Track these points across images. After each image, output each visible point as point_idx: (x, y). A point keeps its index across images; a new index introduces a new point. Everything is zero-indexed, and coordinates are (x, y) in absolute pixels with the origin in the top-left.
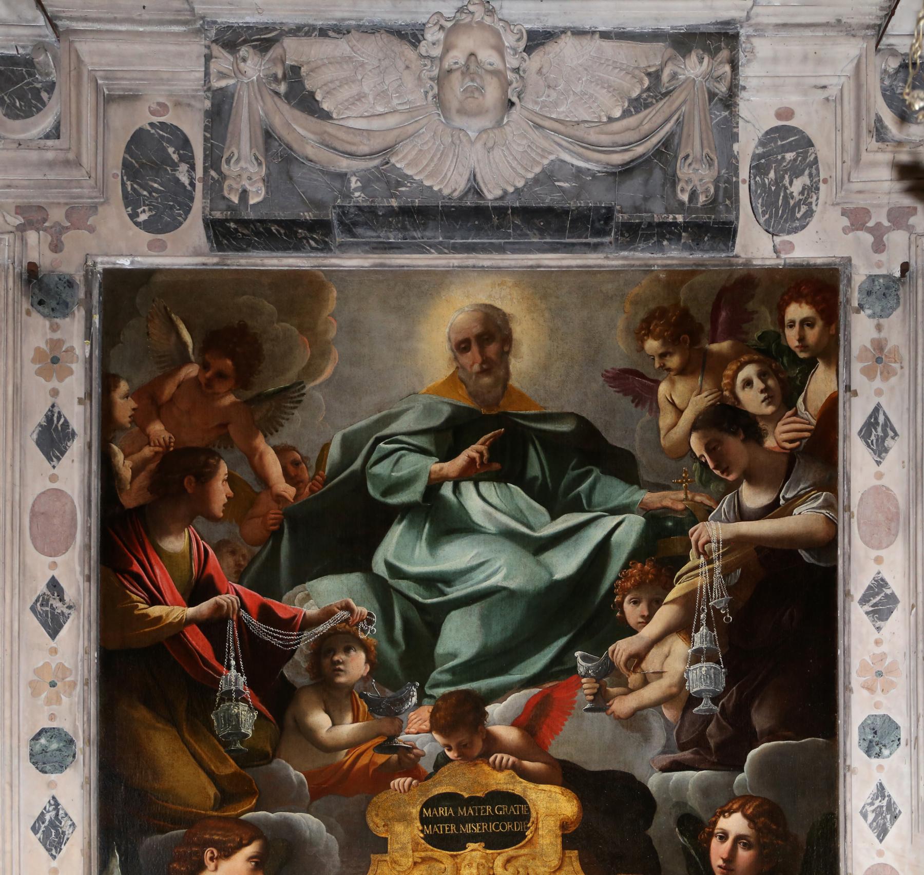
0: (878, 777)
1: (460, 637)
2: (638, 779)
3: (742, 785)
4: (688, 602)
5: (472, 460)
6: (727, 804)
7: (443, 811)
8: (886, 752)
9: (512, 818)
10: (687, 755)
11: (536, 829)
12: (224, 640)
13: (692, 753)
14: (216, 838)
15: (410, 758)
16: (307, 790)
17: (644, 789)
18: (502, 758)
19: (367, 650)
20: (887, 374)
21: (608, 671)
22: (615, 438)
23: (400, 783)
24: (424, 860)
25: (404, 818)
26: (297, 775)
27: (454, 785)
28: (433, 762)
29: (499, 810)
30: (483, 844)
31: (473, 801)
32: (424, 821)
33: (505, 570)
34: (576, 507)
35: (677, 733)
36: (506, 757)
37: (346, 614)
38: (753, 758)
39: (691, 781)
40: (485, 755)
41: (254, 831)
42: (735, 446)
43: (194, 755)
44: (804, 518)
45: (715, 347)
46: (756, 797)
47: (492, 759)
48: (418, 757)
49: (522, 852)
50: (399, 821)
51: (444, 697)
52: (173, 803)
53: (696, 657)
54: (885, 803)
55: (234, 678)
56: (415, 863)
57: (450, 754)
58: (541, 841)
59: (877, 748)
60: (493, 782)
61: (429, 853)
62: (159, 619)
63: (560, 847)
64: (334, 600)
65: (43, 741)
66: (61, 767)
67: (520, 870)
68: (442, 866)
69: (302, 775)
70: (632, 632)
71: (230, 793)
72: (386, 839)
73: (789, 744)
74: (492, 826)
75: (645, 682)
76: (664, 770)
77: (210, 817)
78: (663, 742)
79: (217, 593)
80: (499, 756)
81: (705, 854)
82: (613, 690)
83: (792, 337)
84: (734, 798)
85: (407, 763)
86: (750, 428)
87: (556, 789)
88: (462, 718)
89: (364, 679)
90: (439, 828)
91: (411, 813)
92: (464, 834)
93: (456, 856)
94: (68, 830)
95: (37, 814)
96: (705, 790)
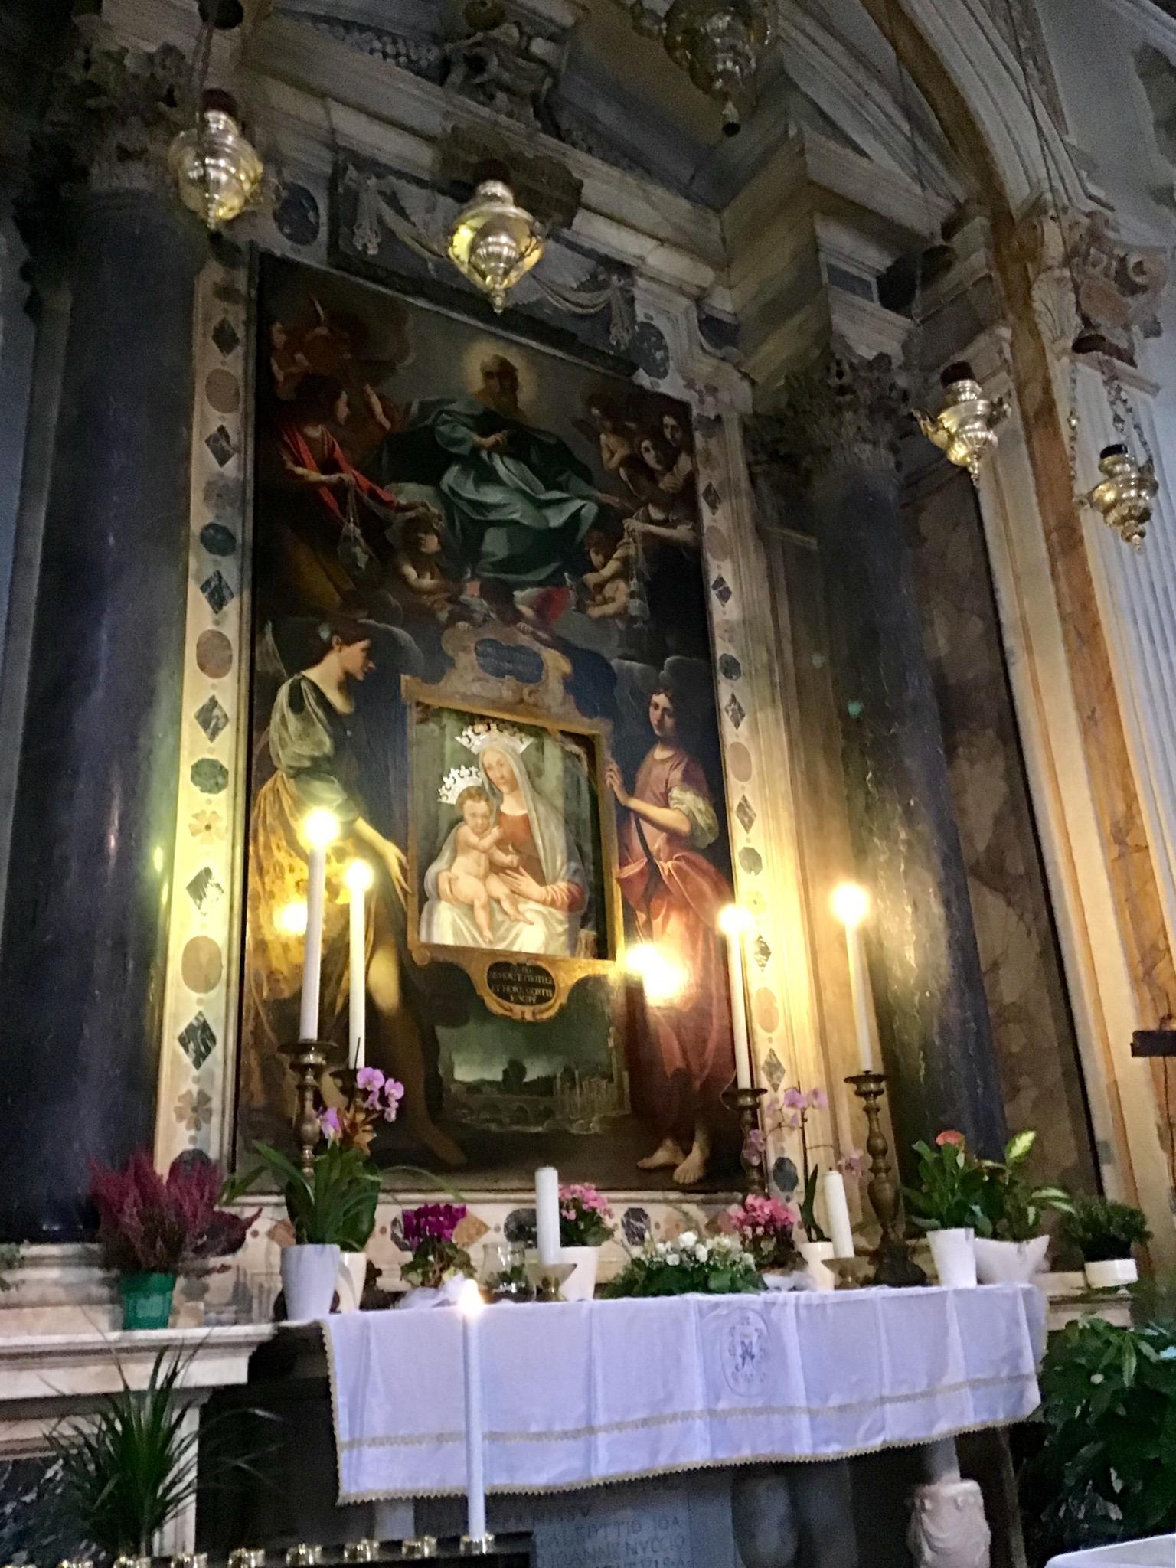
1: (495, 544)
4: (625, 561)
5: (497, 443)
12: (346, 502)
17: (609, 667)
19: (438, 536)
20: (713, 469)
21: (583, 587)
22: (579, 455)
23: (462, 625)
25: (465, 649)
33: (519, 512)
34: (560, 488)
37: (421, 509)
42: (643, 481)
44: (681, 532)
45: (628, 424)
51: (488, 579)
53: (632, 595)
55: (352, 528)
62: (302, 476)
64: (418, 499)
70: (595, 570)
71: (351, 602)
75: (605, 601)
76: (620, 657)
79: (341, 471)
82: (588, 602)
83: (668, 433)
86: (652, 476)
87: (556, 653)
88: (500, 594)
89: (437, 553)
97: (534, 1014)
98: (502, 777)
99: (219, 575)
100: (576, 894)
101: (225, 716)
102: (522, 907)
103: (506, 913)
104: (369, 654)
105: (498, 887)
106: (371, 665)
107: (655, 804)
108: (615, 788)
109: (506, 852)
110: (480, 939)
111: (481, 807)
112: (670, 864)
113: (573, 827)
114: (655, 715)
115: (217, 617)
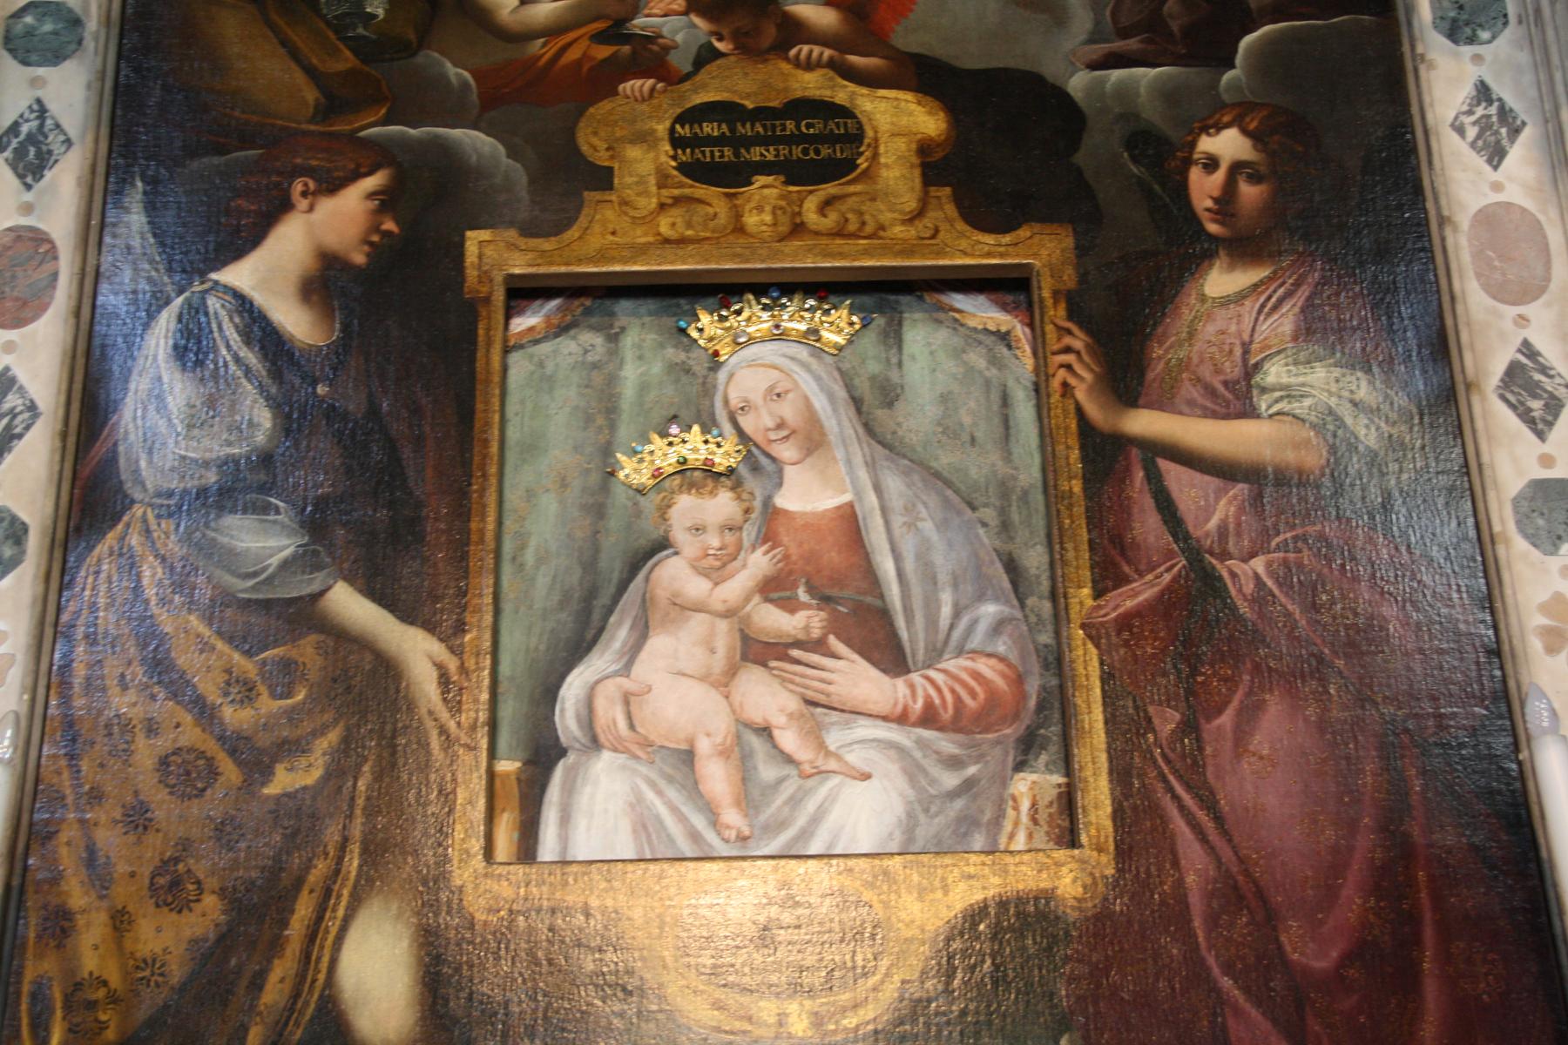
0: (1472, 73)
2: (1050, 80)
3: (1234, 86)
6: (1210, 117)
7: (709, 129)
8: (1485, 35)
9: (832, 139)
10: (1133, 44)
11: (876, 155)
13: (1141, 41)
14: (314, 163)
15: (651, 51)
16: (474, 97)
18: (811, 52)
23: (634, 86)
24: (677, 201)
25: (644, 138)
26: (457, 74)
27: (728, 90)
28: (691, 57)
29: (808, 126)
30: (782, 178)
31: (760, 113)
32: (677, 142)
35: (1113, 14)
36: (817, 50)
38: (1249, 49)
39: (1144, 83)
40: (781, 48)
41: (378, 155)
43: (284, 43)
46: (1263, 105)
47: (793, 52)
48: (666, 49)
49: (852, 189)
50: (632, 142)
52: (243, 112)
54: (1493, 110)
56: (662, 206)
57: (720, 46)
58: (884, 173)
59: (1468, 31)
60: (796, 86)
61: (687, 191)
63: (918, 182)
65: (29, 19)
66: (56, 57)
67: (850, 216)
68: (711, 210)
69: (466, 74)
72: (610, 170)
73: (1314, 26)
74: (797, 152)
76: (1093, 66)
77: (305, 133)
78: (1089, 25)
80: (806, 48)
81: (1181, 191)
84: (1223, 107)
85: (649, 58)
87: (908, 96)
90: (703, 153)
91: (654, 131)
92: (748, 163)
93: (734, 195)
94: (57, 148)
95: (8, 123)
96: (1169, 95)
97: (818, 1020)
98: (781, 425)
99: (41, 110)
100: (1000, 683)
101: (32, 407)
102: (833, 739)
103: (789, 760)
104: (386, 201)
105: (764, 695)
106: (389, 225)
107: (1215, 415)
108: (1081, 394)
109: (790, 606)
110: (710, 836)
111: (721, 505)
112: (1258, 564)
113: (989, 514)
114: (1203, 188)
115: (28, 197)
